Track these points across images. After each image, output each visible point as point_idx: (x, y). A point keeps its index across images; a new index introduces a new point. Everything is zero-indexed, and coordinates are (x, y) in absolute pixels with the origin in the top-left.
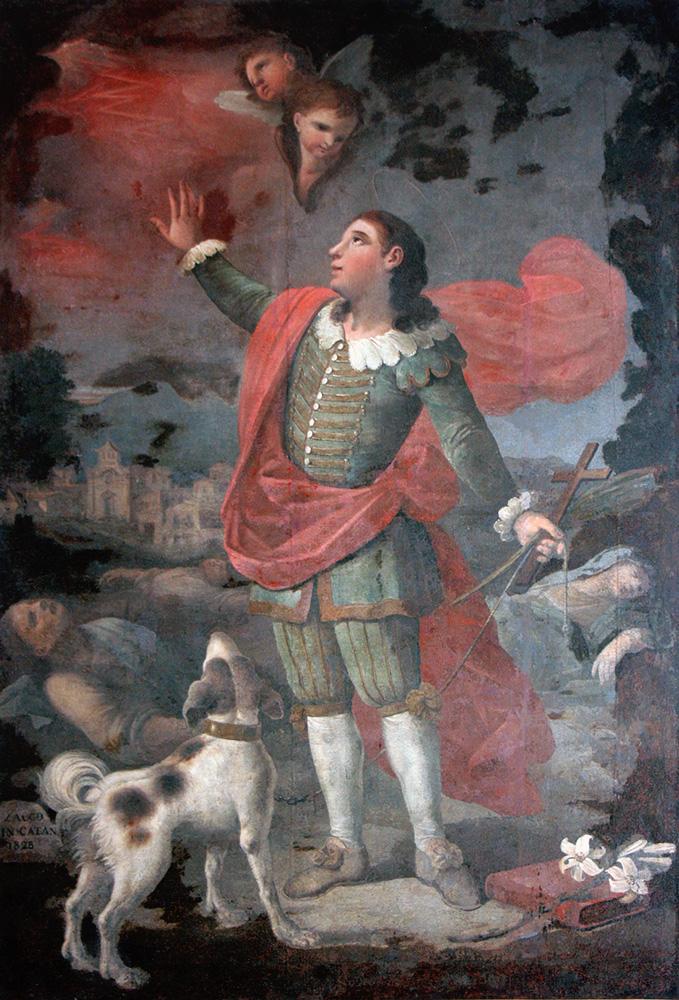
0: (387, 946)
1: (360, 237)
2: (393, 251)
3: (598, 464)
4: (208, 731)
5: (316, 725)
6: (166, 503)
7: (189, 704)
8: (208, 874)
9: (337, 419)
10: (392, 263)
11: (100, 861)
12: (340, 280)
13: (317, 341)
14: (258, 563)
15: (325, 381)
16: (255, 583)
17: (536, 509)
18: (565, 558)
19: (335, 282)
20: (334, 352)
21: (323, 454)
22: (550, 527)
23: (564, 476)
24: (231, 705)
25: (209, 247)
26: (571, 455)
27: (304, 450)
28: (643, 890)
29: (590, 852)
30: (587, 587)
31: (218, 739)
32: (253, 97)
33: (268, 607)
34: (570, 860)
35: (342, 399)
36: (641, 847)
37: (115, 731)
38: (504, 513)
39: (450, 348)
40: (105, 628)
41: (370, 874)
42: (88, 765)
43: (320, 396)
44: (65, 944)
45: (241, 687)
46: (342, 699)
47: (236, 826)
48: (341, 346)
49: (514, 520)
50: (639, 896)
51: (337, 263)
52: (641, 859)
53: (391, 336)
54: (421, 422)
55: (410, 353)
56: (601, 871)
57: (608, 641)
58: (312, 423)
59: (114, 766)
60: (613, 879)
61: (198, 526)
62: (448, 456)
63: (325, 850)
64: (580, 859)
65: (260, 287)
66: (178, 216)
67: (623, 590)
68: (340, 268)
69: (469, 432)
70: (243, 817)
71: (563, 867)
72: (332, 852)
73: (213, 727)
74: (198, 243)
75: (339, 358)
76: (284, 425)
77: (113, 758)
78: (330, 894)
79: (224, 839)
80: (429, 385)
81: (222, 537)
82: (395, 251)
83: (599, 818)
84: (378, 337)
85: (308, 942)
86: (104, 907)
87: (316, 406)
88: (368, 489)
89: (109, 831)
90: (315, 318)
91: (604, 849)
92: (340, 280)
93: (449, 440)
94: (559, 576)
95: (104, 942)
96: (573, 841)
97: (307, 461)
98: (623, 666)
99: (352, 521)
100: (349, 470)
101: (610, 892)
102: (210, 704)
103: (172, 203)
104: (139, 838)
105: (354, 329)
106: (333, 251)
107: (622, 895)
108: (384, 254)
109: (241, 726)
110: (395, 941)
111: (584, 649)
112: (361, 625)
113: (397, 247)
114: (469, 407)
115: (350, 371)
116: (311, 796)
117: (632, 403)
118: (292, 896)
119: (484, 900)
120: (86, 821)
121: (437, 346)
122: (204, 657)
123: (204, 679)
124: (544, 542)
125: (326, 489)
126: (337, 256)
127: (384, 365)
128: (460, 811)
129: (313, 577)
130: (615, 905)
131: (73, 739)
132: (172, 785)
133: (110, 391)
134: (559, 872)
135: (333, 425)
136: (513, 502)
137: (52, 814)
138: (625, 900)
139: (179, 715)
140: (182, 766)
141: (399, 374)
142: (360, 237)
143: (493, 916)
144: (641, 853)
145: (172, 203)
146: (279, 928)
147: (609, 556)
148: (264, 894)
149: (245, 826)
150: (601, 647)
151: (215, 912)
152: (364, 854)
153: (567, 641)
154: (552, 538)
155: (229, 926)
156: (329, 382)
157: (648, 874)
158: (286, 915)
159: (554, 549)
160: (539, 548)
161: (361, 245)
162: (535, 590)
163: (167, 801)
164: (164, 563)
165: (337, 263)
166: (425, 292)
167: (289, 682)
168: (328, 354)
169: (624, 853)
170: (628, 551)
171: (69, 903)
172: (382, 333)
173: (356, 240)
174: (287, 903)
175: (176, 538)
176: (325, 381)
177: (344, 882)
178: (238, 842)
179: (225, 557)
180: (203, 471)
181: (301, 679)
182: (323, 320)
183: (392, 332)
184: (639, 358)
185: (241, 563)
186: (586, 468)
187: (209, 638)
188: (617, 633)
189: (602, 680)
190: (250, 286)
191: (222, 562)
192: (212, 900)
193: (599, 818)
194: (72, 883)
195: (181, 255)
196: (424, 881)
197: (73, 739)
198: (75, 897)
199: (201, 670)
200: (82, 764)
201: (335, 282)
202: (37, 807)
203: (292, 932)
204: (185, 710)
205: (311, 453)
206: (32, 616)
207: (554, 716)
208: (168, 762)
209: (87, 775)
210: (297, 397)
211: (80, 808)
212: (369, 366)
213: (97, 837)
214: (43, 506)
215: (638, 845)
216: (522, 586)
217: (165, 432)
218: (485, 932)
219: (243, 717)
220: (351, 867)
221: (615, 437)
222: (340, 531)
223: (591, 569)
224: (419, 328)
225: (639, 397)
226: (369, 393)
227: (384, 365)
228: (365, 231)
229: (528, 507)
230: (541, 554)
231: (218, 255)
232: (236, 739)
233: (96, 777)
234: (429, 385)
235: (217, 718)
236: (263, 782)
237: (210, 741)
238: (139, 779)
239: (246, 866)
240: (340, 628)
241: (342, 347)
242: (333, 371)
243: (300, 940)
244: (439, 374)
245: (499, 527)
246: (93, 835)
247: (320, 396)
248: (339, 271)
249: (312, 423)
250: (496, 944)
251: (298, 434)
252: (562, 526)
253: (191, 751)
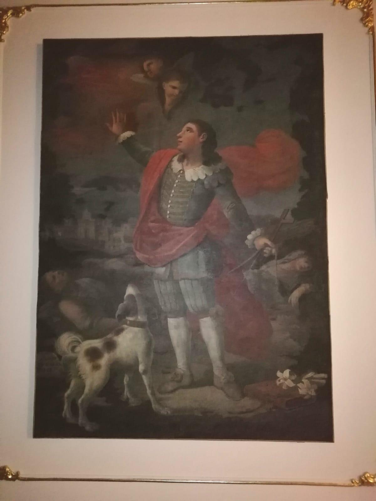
0: (202, 415)
1: (189, 129)
2: (202, 135)
3: (289, 218)
4: (126, 324)
5: (172, 322)
6: (110, 232)
7: (118, 312)
8: (125, 383)
9: (180, 200)
10: (202, 139)
11: (80, 377)
12: (182, 146)
13: (172, 170)
14: (147, 256)
15: (175, 185)
16: (147, 264)
17: (262, 235)
18: (276, 255)
19: (179, 147)
20: (179, 174)
21: (174, 214)
22: (269, 243)
23: (275, 221)
24: (135, 313)
25: (128, 134)
26: (277, 214)
27: (167, 212)
28: (313, 393)
29: (289, 377)
30: (286, 266)
31: (130, 327)
32: (146, 77)
33: (152, 273)
34: (281, 380)
35: (182, 192)
36: (312, 375)
37: (87, 323)
38: (250, 237)
39: (227, 172)
40: (84, 282)
41: (193, 384)
42: (75, 337)
43: (173, 191)
45: (140, 307)
46: (183, 312)
47: (137, 363)
48: (182, 172)
49: (254, 240)
50: (311, 396)
51: (180, 140)
52: (313, 380)
53: (202, 168)
54: (215, 201)
55: (210, 174)
56: (295, 385)
57: (295, 288)
58: (170, 201)
60: (300, 388)
61: (123, 242)
62: (226, 214)
63: (175, 374)
64: (285, 379)
65: (149, 149)
66: (116, 122)
67: (301, 268)
68: (181, 142)
69: (234, 205)
70: (140, 359)
71: (278, 383)
72: (178, 375)
73: (128, 322)
74: (124, 132)
75: (181, 176)
76: (159, 202)
77: (87, 335)
78: (177, 392)
79: (132, 368)
80: (218, 186)
81: (133, 246)
82: (203, 135)
83: (294, 362)
84: (197, 168)
85: (168, 413)
86: (81, 396)
87: (172, 195)
88: (193, 228)
89: (84, 364)
90: (171, 161)
91: (296, 376)
92: (182, 146)
93: (226, 208)
94: (274, 262)
95: (80, 412)
96: (282, 372)
97: (168, 217)
98: (302, 298)
99: (186, 240)
100: (185, 220)
101: (299, 394)
102: (127, 312)
103: (114, 118)
104: (96, 367)
105: (187, 165)
106: (178, 135)
107: (304, 395)
108: (199, 135)
109: (139, 322)
110: (205, 412)
111: (285, 291)
112: (190, 281)
113: (204, 133)
114: (234, 195)
115: (186, 181)
116: (169, 350)
117: (303, 193)
118: (161, 393)
119: (243, 395)
120: (74, 360)
121: (221, 171)
122: (125, 294)
123: (125, 302)
124: (267, 248)
125: (176, 228)
126: (180, 137)
127: (199, 179)
128: (232, 358)
129: (170, 262)
130: (301, 399)
131: (69, 326)
132: (111, 346)
133: (87, 189)
134: (276, 384)
135: (178, 202)
136: (253, 233)
137: (60, 357)
138: (306, 397)
139: (114, 317)
140: (115, 338)
141: (206, 182)
142: (189, 129)
143: (247, 403)
144: (312, 378)
145: (114, 118)
146: (154, 406)
147: (295, 254)
148: (149, 392)
149: (141, 363)
150: (292, 291)
151: (128, 399)
152: (192, 375)
153: (277, 288)
154: (270, 247)
155: (133, 405)
156: (177, 186)
157: (316, 387)
158: (159, 401)
159: (271, 251)
160: (265, 251)
161: (190, 132)
162: (264, 268)
163: (109, 352)
164: (109, 256)
165: (180, 140)
166: (216, 150)
167: (160, 304)
168: (176, 175)
169: (304, 378)
170: (303, 252)
172: (199, 167)
173: (188, 131)
174: (159, 396)
175: (114, 246)
176: (175, 185)
177: (184, 387)
178: (138, 370)
179: (134, 254)
180: (125, 221)
181: (165, 303)
182: (174, 162)
183: (202, 166)
184: (306, 175)
185: (140, 256)
186: (284, 219)
187: (127, 286)
188: (298, 285)
189: (293, 305)
190: (144, 149)
191: (133, 256)
192: (127, 393)
193: (294, 362)
194: (68, 386)
195: (117, 137)
196: (218, 388)
197: (69, 326)
198: (69, 392)
199: (124, 299)
200: (73, 337)
201: (179, 147)
202: (54, 355)
203: (161, 408)
204: (117, 315)
205: (170, 213)
206: (54, 277)
207: (274, 319)
208: (109, 336)
209: (75, 341)
210: (164, 192)
211: (71, 354)
212: (193, 179)
213: (79, 367)
214: (60, 234)
215: (310, 375)
216: (258, 266)
217: (110, 205)
218: (244, 410)
219: (141, 318)
220: (186, 381)
221: (296, 206)
222: (182, 244)
223: (288, 259)
224: (214, 164)
225: (306, 191)
226: (193, 190)
227: (199, 179)
228: (190, 127)
229: (260, 234)
230: (265, 253)
231: (132, 137)
232: (138, 327)
233: (79, 343)
234: (218, 186)
235: (131, 319)
236: (149, 345)
237: (126, 328)
238: (97, 343)
239: (142, 379)
240: (182, 284)
241: (182, 172)
242: (178, 182)
243: (164, 412)
244: (221, 182)
245: (248, 243)
246: (77, 366)
247: (173, 191)
248: (181, 143)
249: (170, 201)
250: (250, 415)
251: (164, 206)
252: (274, 241)
253: (119, 331)
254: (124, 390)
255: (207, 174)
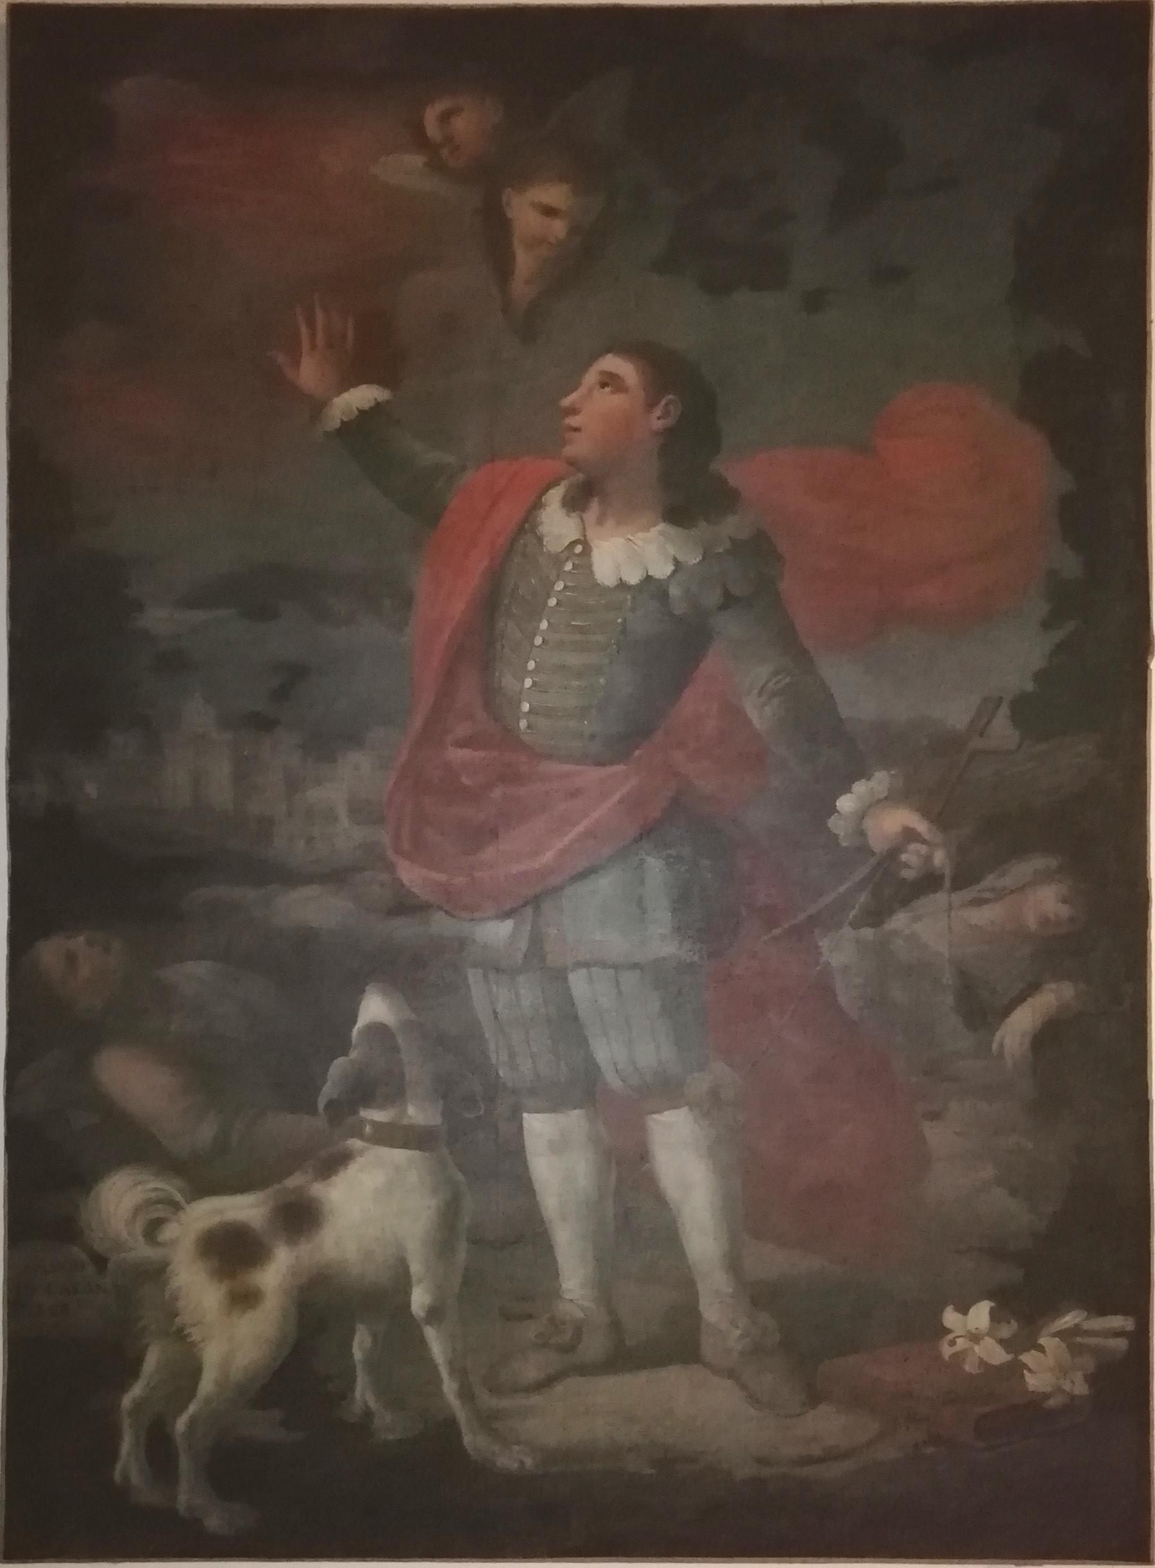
1: (610, 381)
2: (663, 402)
3: (1002, 731)
4: (360, 1135)
6: (293, 785)
7: (328, 1091)
8: (358, 1354)
9: (574, 660)
10: (661, 422)
11: (180, 1335)
12: (579, 447)
13: (540, 539)
14: (441, 877)
15: (552, 602)
16: (440, 908)
18: (947, 872)
19: (569, 451)
21: (549, 713)
22: (921, 826)
25: (362, 396)
27: (519, 706)
28: (1080, 1388)
30: (983, 916)
32: (436, 165)
33: (462, 943)
34: (959, 1341)
35: (580, 630)
36: (1077, 1321)
37: (207, 1132)
38: (846, 803)
42: (159, 1186)
43: (544, 625)
44: (119, 1467)
47: (403, 1281)
48: (579, 549)
49: (862, 815)
50: (1073, 1398)
51: (573, 421)
52: (1079, 1339)
53: (661, 533)
54: (711, 664)
55: (692, 558)
58: (531, 665)
59: (203, 1188)
60: (1030, 1370)
61: (345, 822)
63: (552, 1320)
64: (975, 1338)
65: (449, 459)
66: (313, 347)
67: (1045, 921)
68: (576, 430)
69: (788, 680)
70: (416, 1267)
71: (947, 1351)
72: (564, 1323)
73: (368, 1129)
74: (347, 389)
78: (559, 1388)
81: (384, 837)
82: (666, 405)
84: (641, 535)
85: (522, 1463)
86: (185, 1407)
87: (538, 641)
90: (537, 505)
91: (1014, 1325)
92: (579, 447)
93: (756, 691)
94: (940, 898)
95: (185, 1464)
97: (523, 724)
99: (596, 815)
100: (593, 737)
103: (304, 330)
105: (600, 521)
106: (566, 402)
107: (1046, 1396)
108: (651, 405)
109: (410, 1128)
112: (612, 971)
113: (671, 397)
115: (596, 587)
117: (1058, 635)
118: (496, 1390)
119: (814, 1397)
120: (158, 1272)
121: (737, 547)
122: (355, 1022)
123: (354, 1054)
124: (913, 847)
126: (573, 411)
127: (648, 579)
130: (1033, 1407)
133: (199, 616)
134: (938, 1357)
135: (563, 667)
136: (860, 787)
137: (100, 1261)
138: (1052, 1403)
139: (312, 1110)
140: (318, 1189)
141: (674, 591)
142: (610, 381)
144: (1076, 1330)
145: (304, 330)
146: (472, 1440)
148: (449, 1387)
149: (420, 1281)
151: (368, 1414)
152: (616, 1326)
153: (950, 1000)
155: (391, 1437)
157: (1089, 1363)
158: (487, 1421)
159: (928, 859)
160: (904, 857)
161: (612, 393)
162: (899, 921)
164: (291, 878)
165: (573, 421)
166: (719, 466)
167: (494, 1061)
168: (557, 561)
169: (1045, 1331)
170: (1053, 862)
171: (127, 1401)
172: (647, 529)
173: (603, 385)
175: (310, 840)
176: (552, 602)
177: (584, 1370)
179: (391, 867)
180: (353, 739)
181: (512, 1056)
183: (662, 526)
184: (1070, 564)
185: (411, 875)
186: (981, 735)
187: (363, 991)
188: (1032, 988)
189: (1009, 1062)
190: (428, 456)
191: (384, 876)
192: (363, 1393)
194: (133, 1369)
195: (318, 407)
198: (137, 1391)
200: (152, 1185)
201: (569, 451)
202: (76, 1251)
203: (496, 1448)
204: (322, 1102)
205: (531, 711)
206: (71, 959)
207: (935, 1116)
208: (293, 1182)
210: (510, 629)
211: (143, 1251)
215: (1069, 1320)
216: (876, 916)
218: (816, 1451)
220: (594, 1346)
221: (1029, 686)
222: (580, 828)
223: (992, 890)
224: (708, 522)
225: (1071, 626)
226: (625, 620)
227: (648, 579)
228: (614, 370)
229: (885, 794)
230: (907, 865)
231: (378, 408)
232: (405, 1146)
233: (176, 1207)
234: (723, 607)
235: (379, 1116)
237: (361, 1152)
239: (423, 1342)
240: (578, 982)
241: (582, 548)
242: (565, 587)
243: (508, 1460)
245: (835, 824)
246: (167, 1295)
247: (544, 625)
248: (577, 434)
249: (531, 665)
251: (508, 681)
252: (941, 820)
254: (355, 1381)
255: (680, 558)
